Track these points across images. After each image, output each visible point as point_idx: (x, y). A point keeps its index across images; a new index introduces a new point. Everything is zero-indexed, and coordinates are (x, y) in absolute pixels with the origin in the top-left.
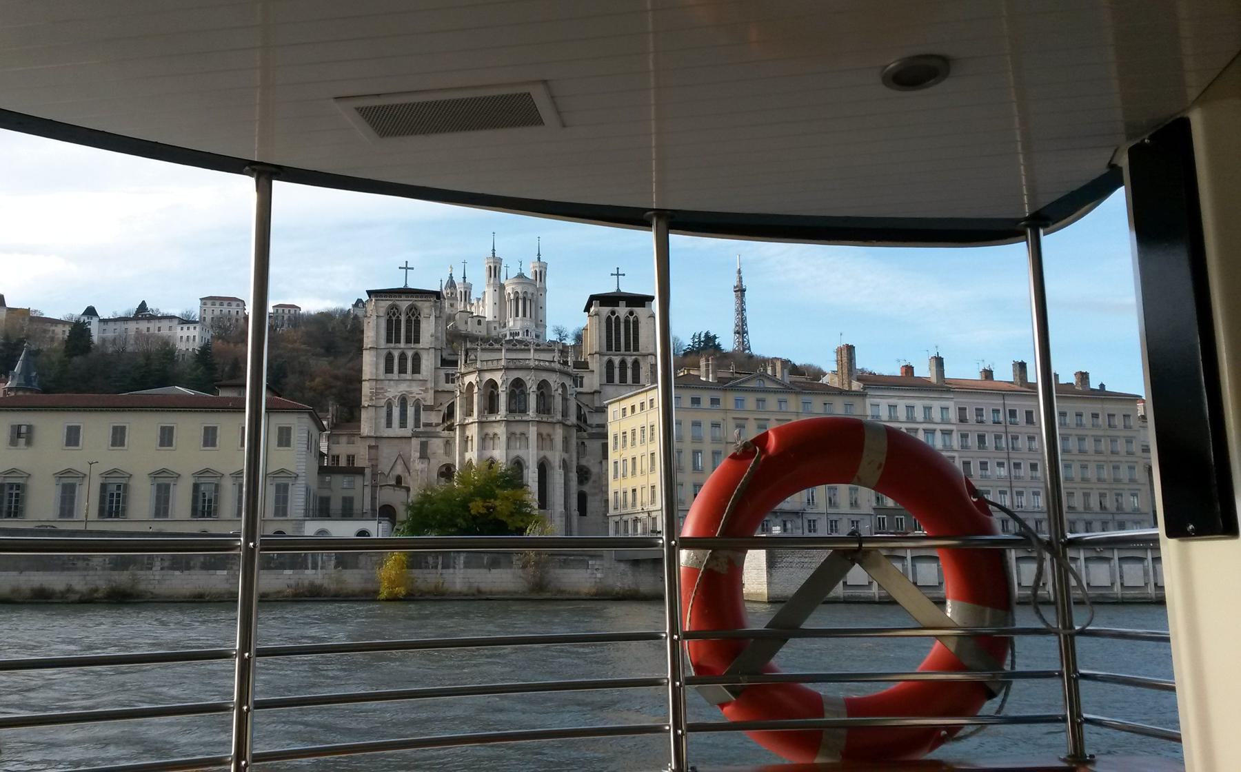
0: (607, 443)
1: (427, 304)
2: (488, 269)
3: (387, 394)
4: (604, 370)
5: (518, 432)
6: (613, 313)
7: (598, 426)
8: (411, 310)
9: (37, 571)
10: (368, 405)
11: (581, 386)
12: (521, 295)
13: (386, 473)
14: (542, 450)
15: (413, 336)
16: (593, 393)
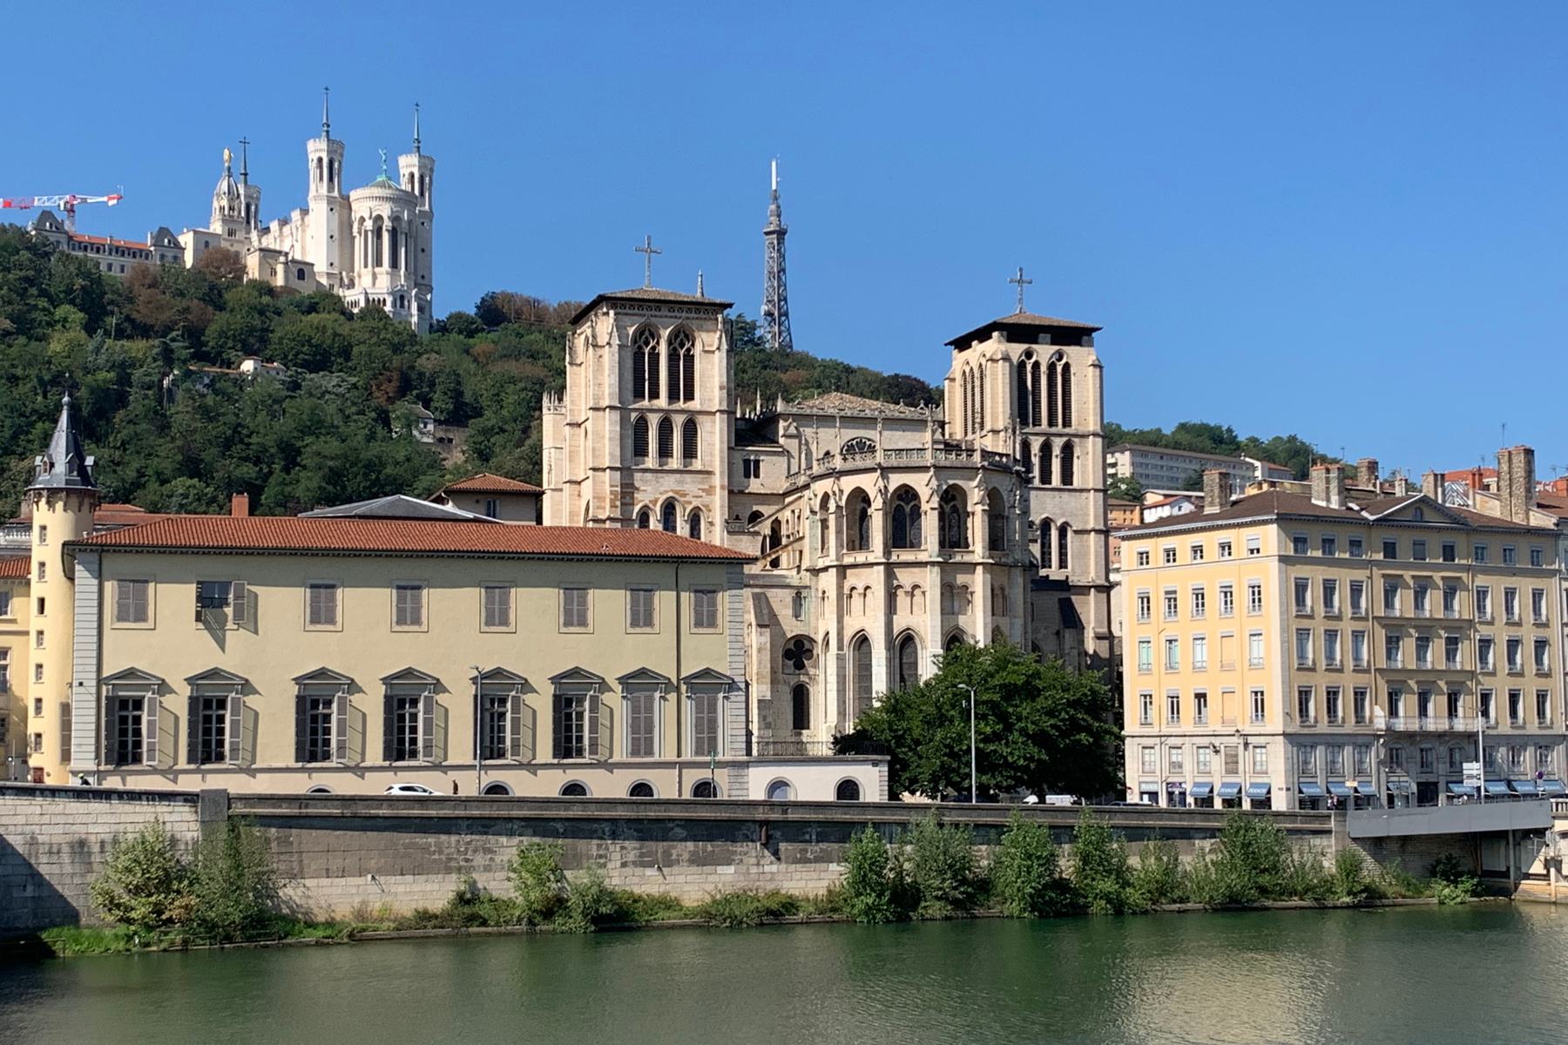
6: (1029, 354)
9: (402, 874)
15: (683, 386)
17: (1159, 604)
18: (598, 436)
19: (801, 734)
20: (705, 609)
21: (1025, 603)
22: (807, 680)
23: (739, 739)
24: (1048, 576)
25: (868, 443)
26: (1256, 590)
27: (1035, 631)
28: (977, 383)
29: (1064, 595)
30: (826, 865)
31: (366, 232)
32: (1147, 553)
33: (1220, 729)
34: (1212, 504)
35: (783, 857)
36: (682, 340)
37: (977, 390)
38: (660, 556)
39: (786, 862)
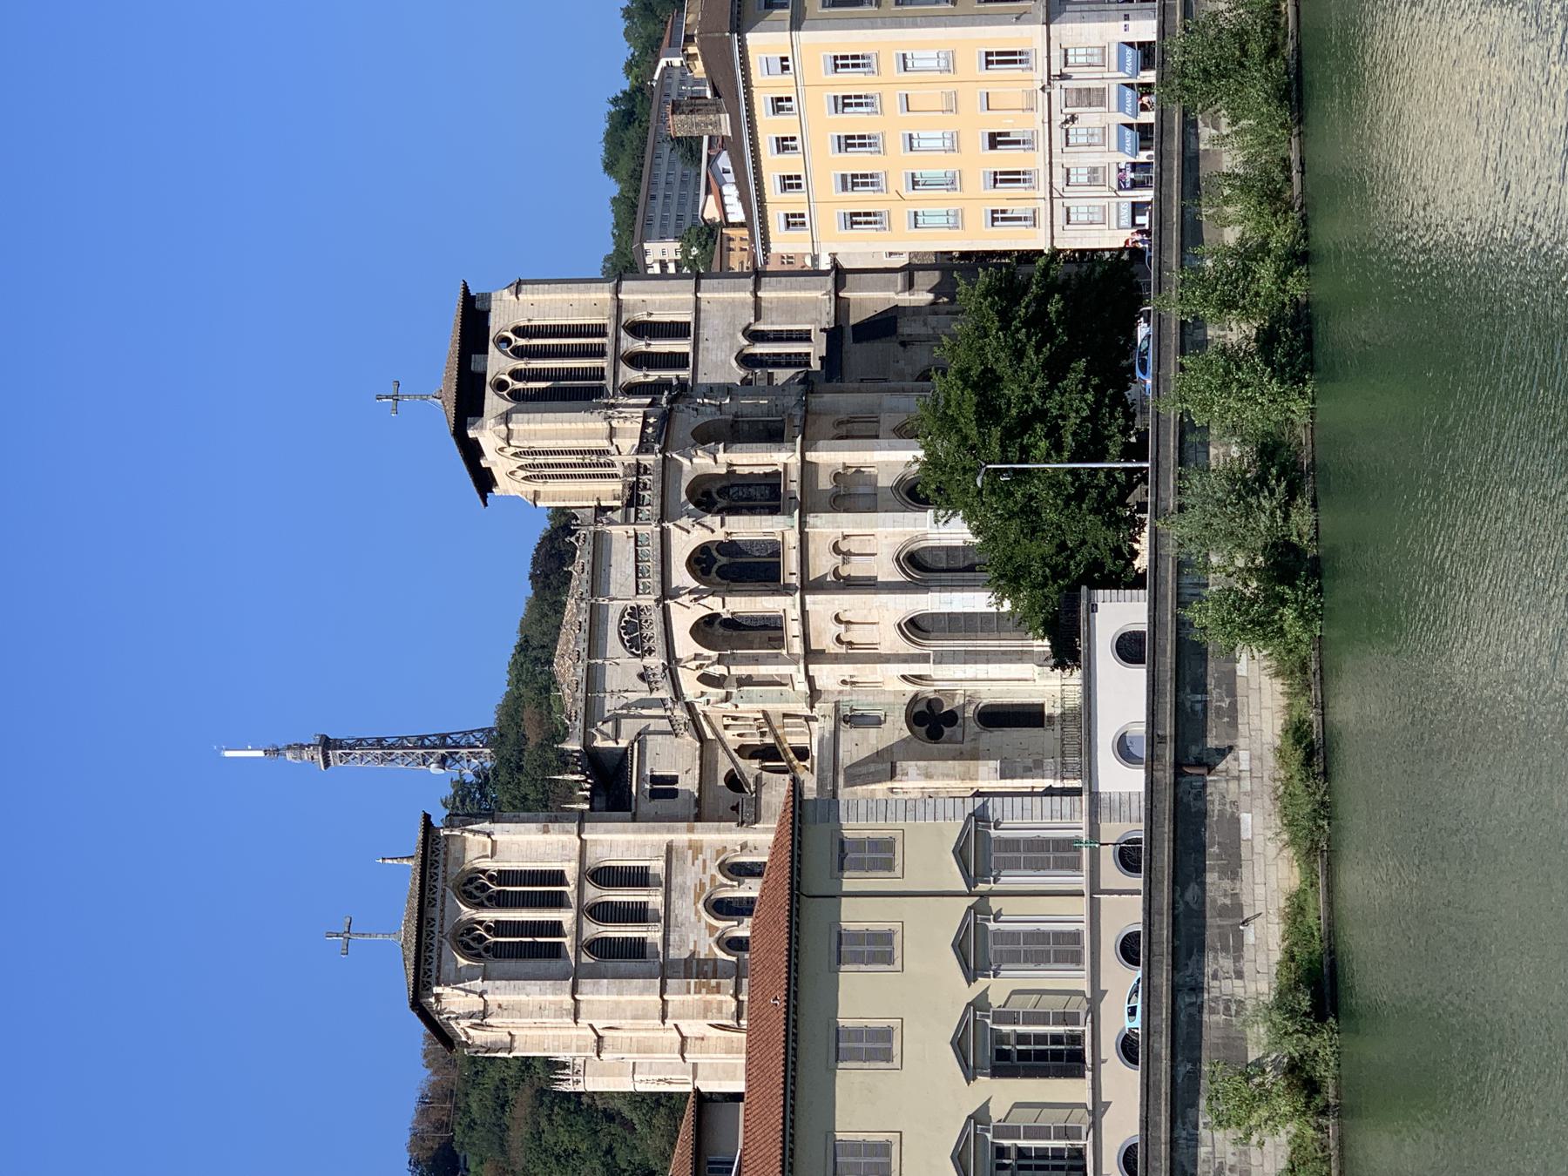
6: (501, 386)
17: (861, 200)
18: (617, 1010)
19: (1051, 717)
20: (867, 855)
21: (859, 391)
22: (973, 707)
23: (1057, 807)
24: (821, 358)
25: (627, 618)
26: (841, 63)
27: (901, 376)
28: (541, 460)
29: (848, 334)
30: (1238, 680)
32: (787, 215)
33: (1041, 114)
34: (717, 124)
35: (1227, 743)
36: (477, 888)
37: (551, 459)
38: (790, 921)
39: (1236, 737)
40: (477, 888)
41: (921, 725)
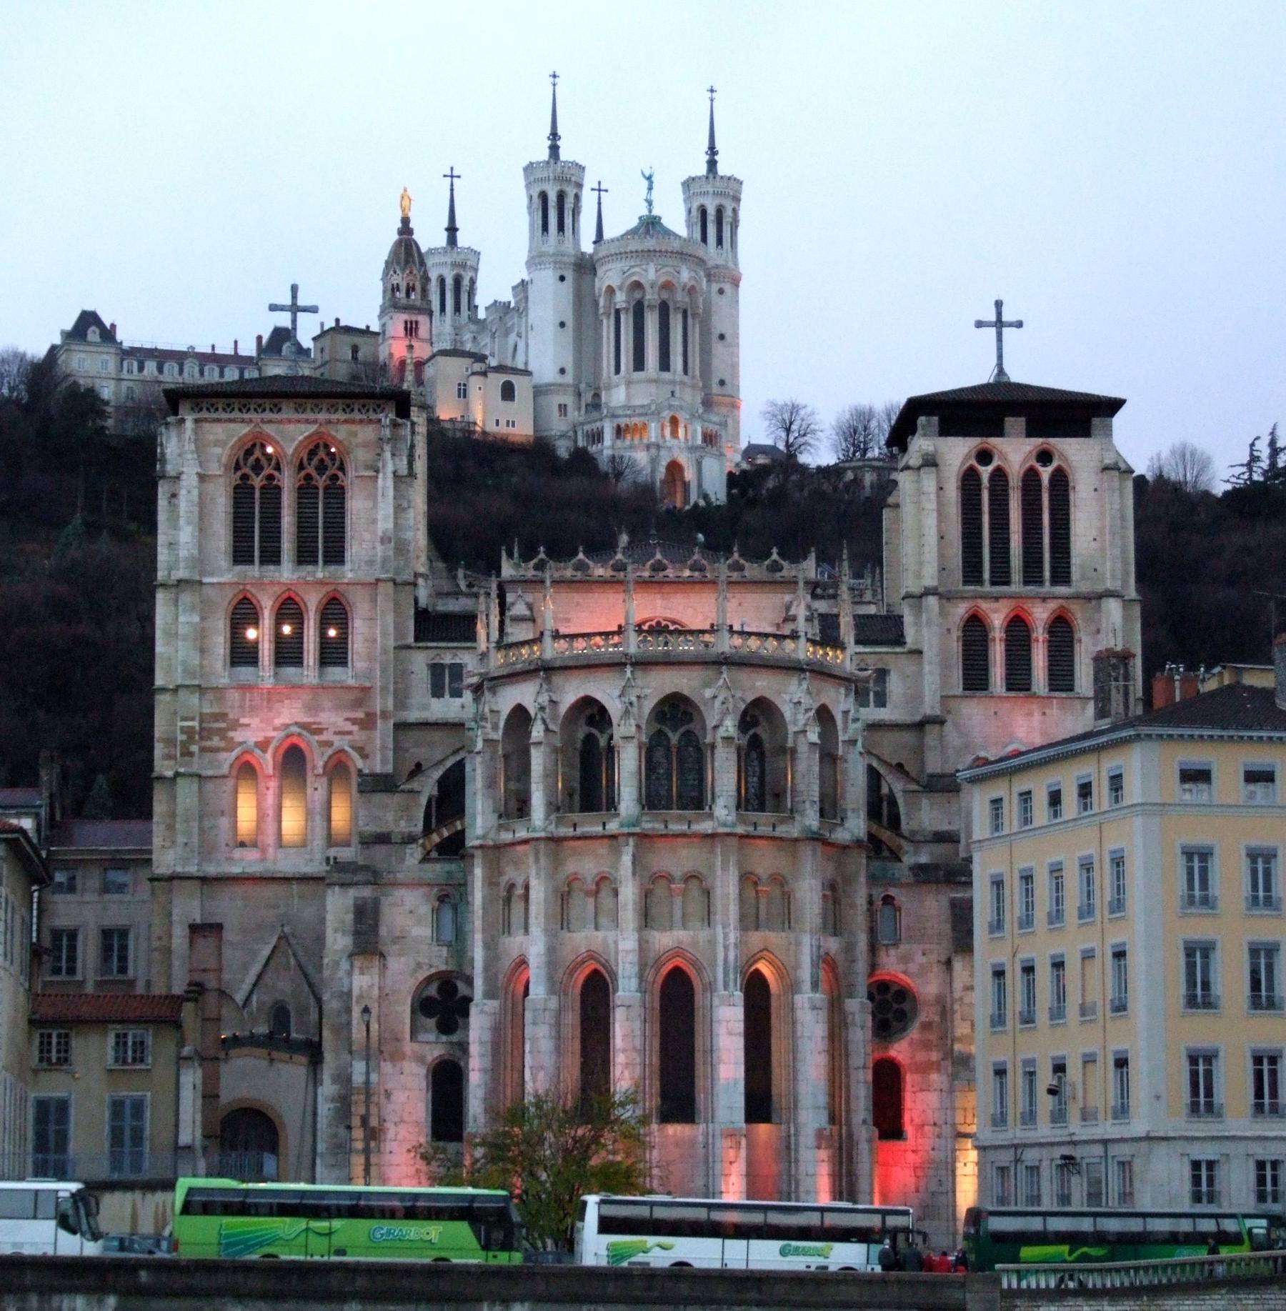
0: (970, 901)
1: (367, 433)
2: (537, 202)
3: (238, 736)
4: (956, 647)
5: (678, 873)
6: (984, 456)
7: (942, 838)
8: (312, 453)
10: (177, 774)
11: (881, 701)
12: (651, 297)
13: (239, 997)
14: (757, 928)
16: (920, 726)
31: (618, 312)
36: (322, 461)
40: (322, 461)
41: (440, 990)
